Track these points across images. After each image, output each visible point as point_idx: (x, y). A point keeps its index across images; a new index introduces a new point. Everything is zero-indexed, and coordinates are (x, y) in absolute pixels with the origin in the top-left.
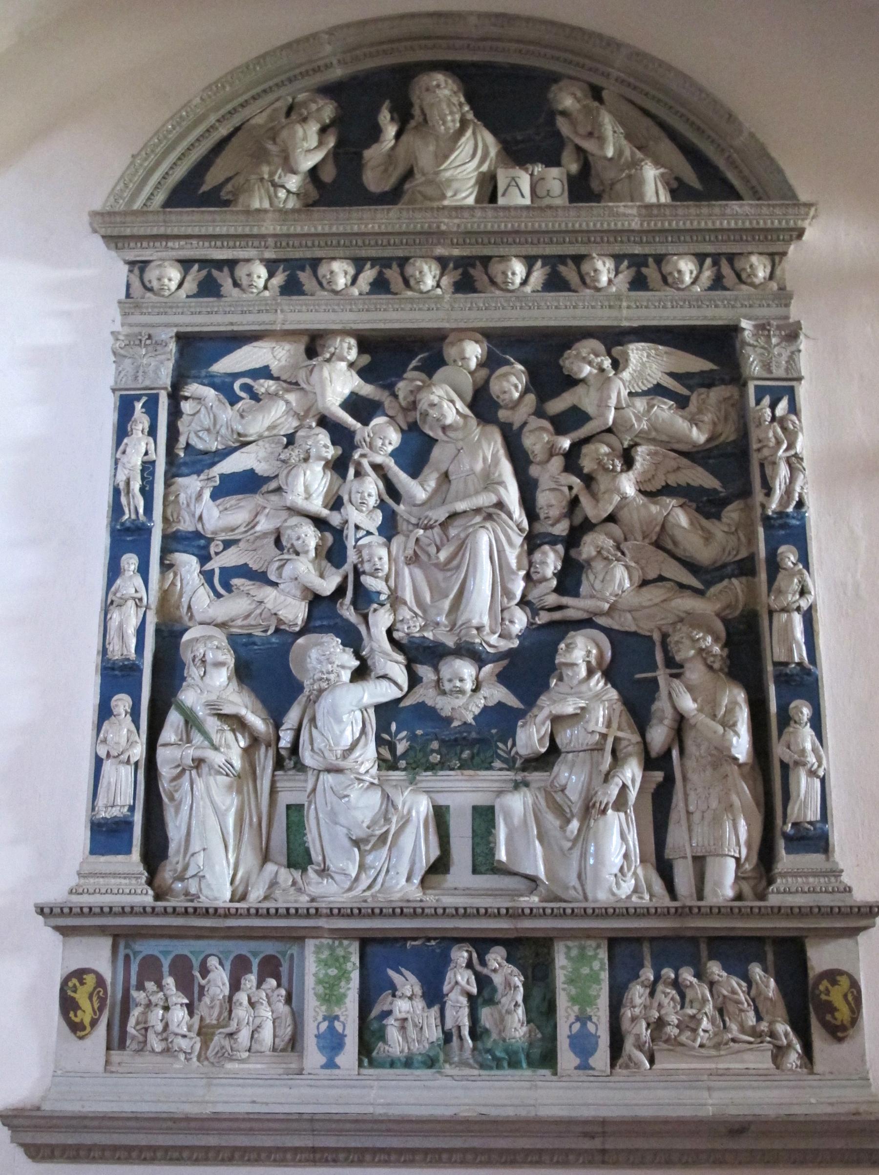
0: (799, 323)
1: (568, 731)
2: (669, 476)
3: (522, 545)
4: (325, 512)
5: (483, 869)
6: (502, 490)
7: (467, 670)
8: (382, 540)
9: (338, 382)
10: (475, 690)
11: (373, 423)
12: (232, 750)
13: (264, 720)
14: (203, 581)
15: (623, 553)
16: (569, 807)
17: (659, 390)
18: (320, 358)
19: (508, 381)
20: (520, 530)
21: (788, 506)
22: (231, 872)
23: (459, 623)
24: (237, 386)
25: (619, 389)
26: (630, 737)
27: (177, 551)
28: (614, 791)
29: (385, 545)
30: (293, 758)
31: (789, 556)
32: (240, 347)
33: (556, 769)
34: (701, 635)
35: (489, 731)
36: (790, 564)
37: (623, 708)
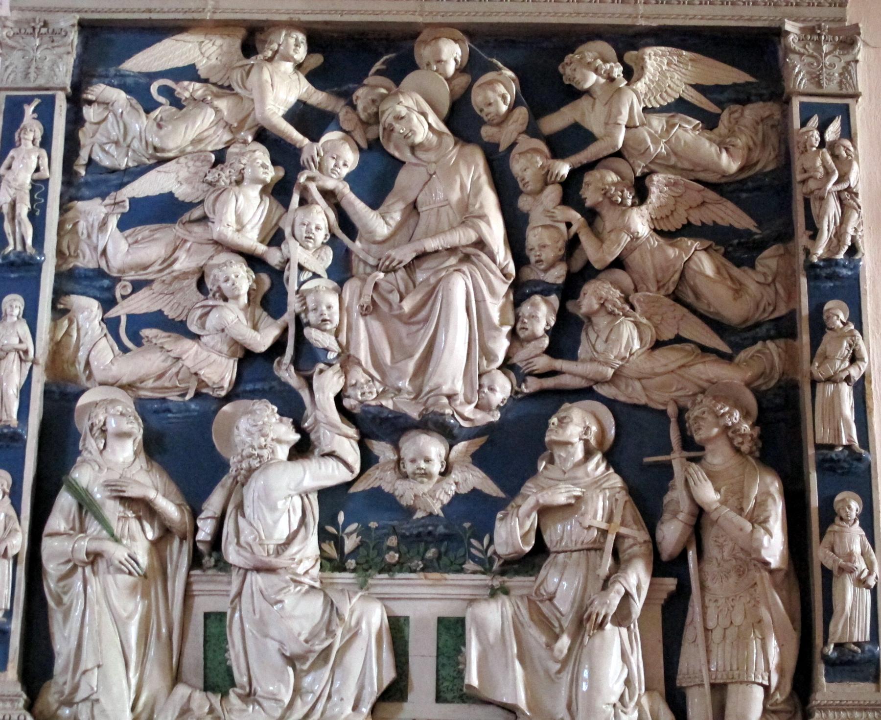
0: (857, 25)
1: (559, 526)
2: (691, 211)
3: (507, 295)
4: (261, 249)
5: (449, 696)
6: (483, 225)
7: (434, 448)
8: (333, 284)
9: (282, 87)
10: (445, 473)
11: (324, 139)
12: (137, 542)
13: (179, 506)
14: (106, 331)
15: (633, 308)
16: (559, 620)
17: (681, 106)
18: (260, 57)
19: (494, 91)
20: (505, 275)
21: (837, 253)
22: (133, 697)
23: (426, 389)
24: (154, 89)
25: (631, 103)
26: (636, 534)
27: (73, 293)
28: (614, 600)
29: (335, 290)
30: (214, 554)
31: (838, 313)
32: (160, 40)
33: (543, 572)
34: (727, 409)
35: (460, 525)
36: (839, 323)
37: (627, 498)
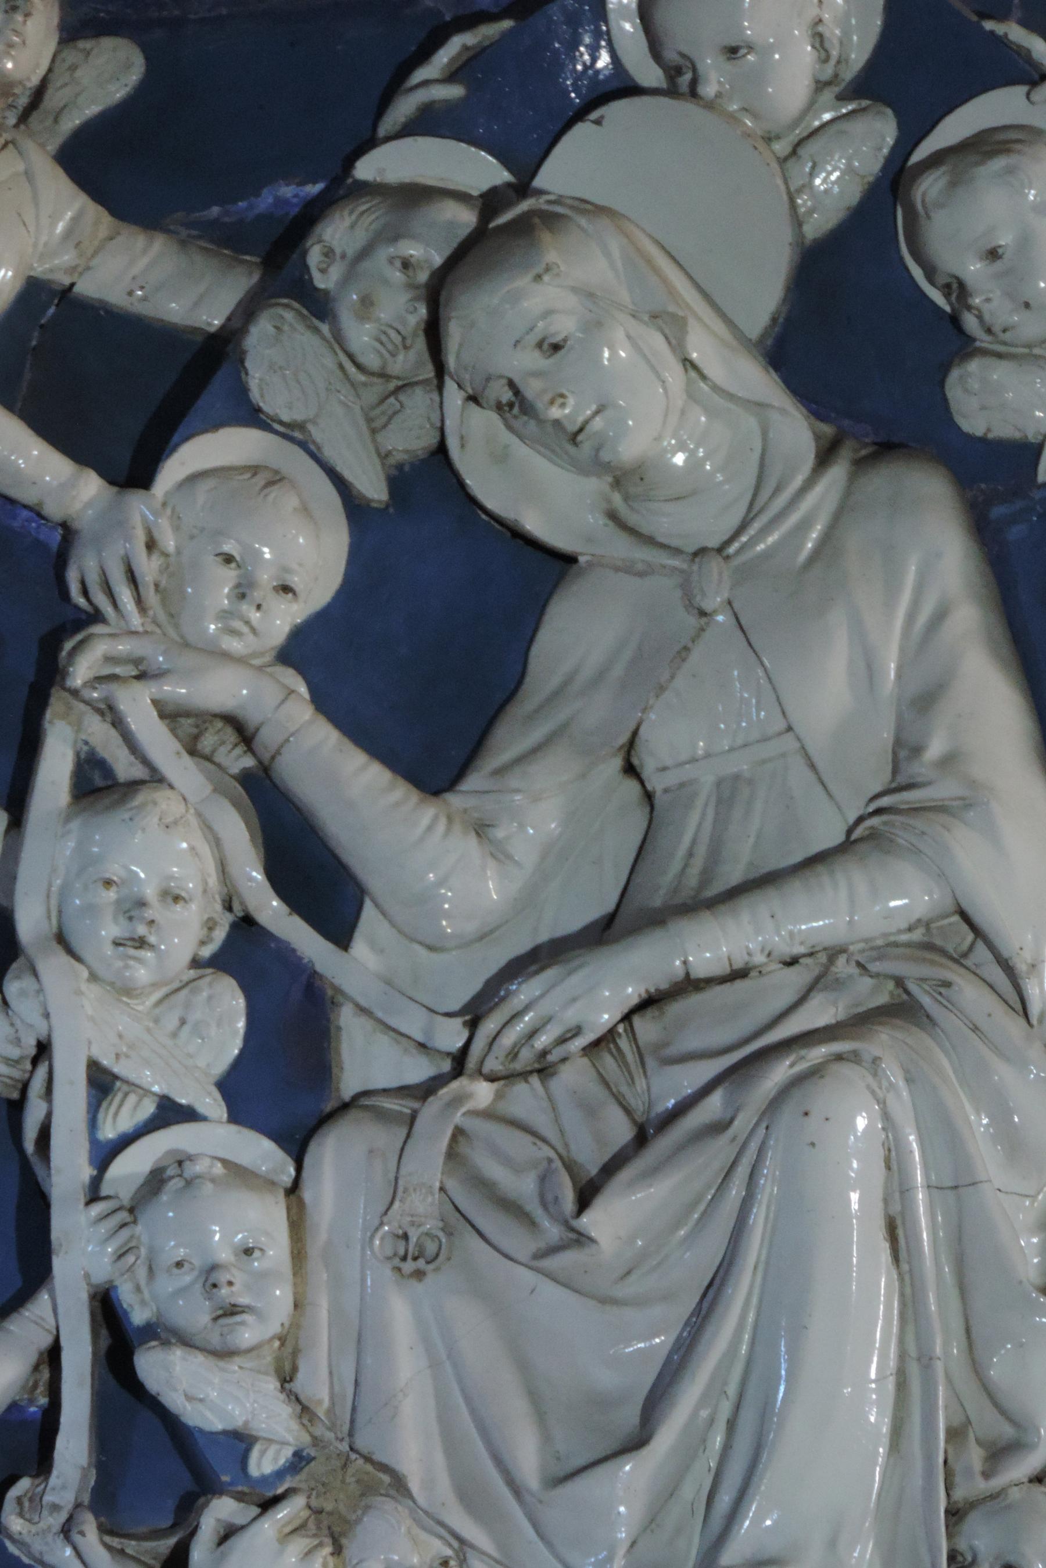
8: (260, 1151)
11: (173, 470)
